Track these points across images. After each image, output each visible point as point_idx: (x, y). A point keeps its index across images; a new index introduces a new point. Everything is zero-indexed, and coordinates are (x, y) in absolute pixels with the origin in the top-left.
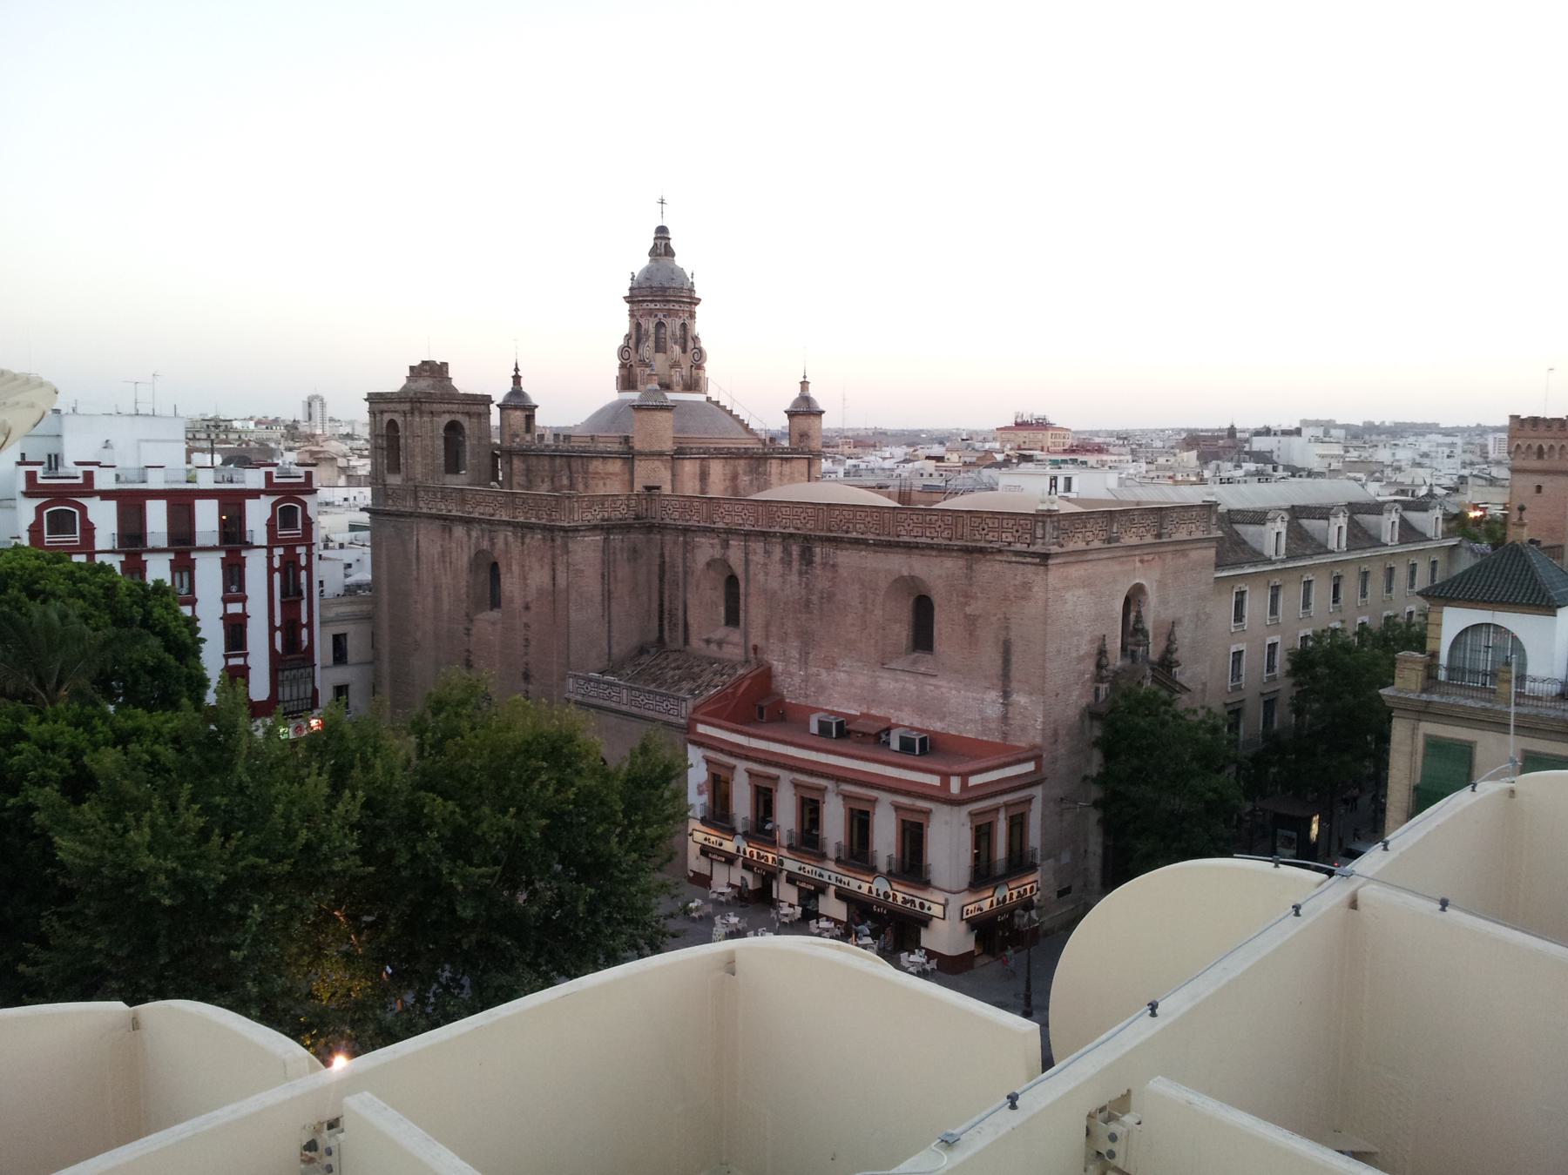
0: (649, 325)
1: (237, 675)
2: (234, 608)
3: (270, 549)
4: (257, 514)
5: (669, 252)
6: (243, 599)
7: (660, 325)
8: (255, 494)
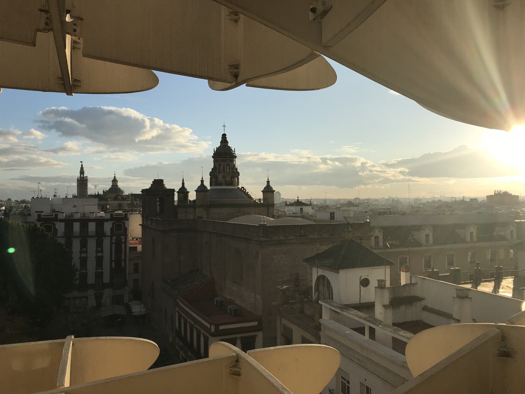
0: (217, 165)
1: (99, 276)
2: (100, 254)
3: (111, 237)
4: (108, 227)
5: (227, 142)
6: (102, 251)
7: (220, 165)
8: (107, 220)
